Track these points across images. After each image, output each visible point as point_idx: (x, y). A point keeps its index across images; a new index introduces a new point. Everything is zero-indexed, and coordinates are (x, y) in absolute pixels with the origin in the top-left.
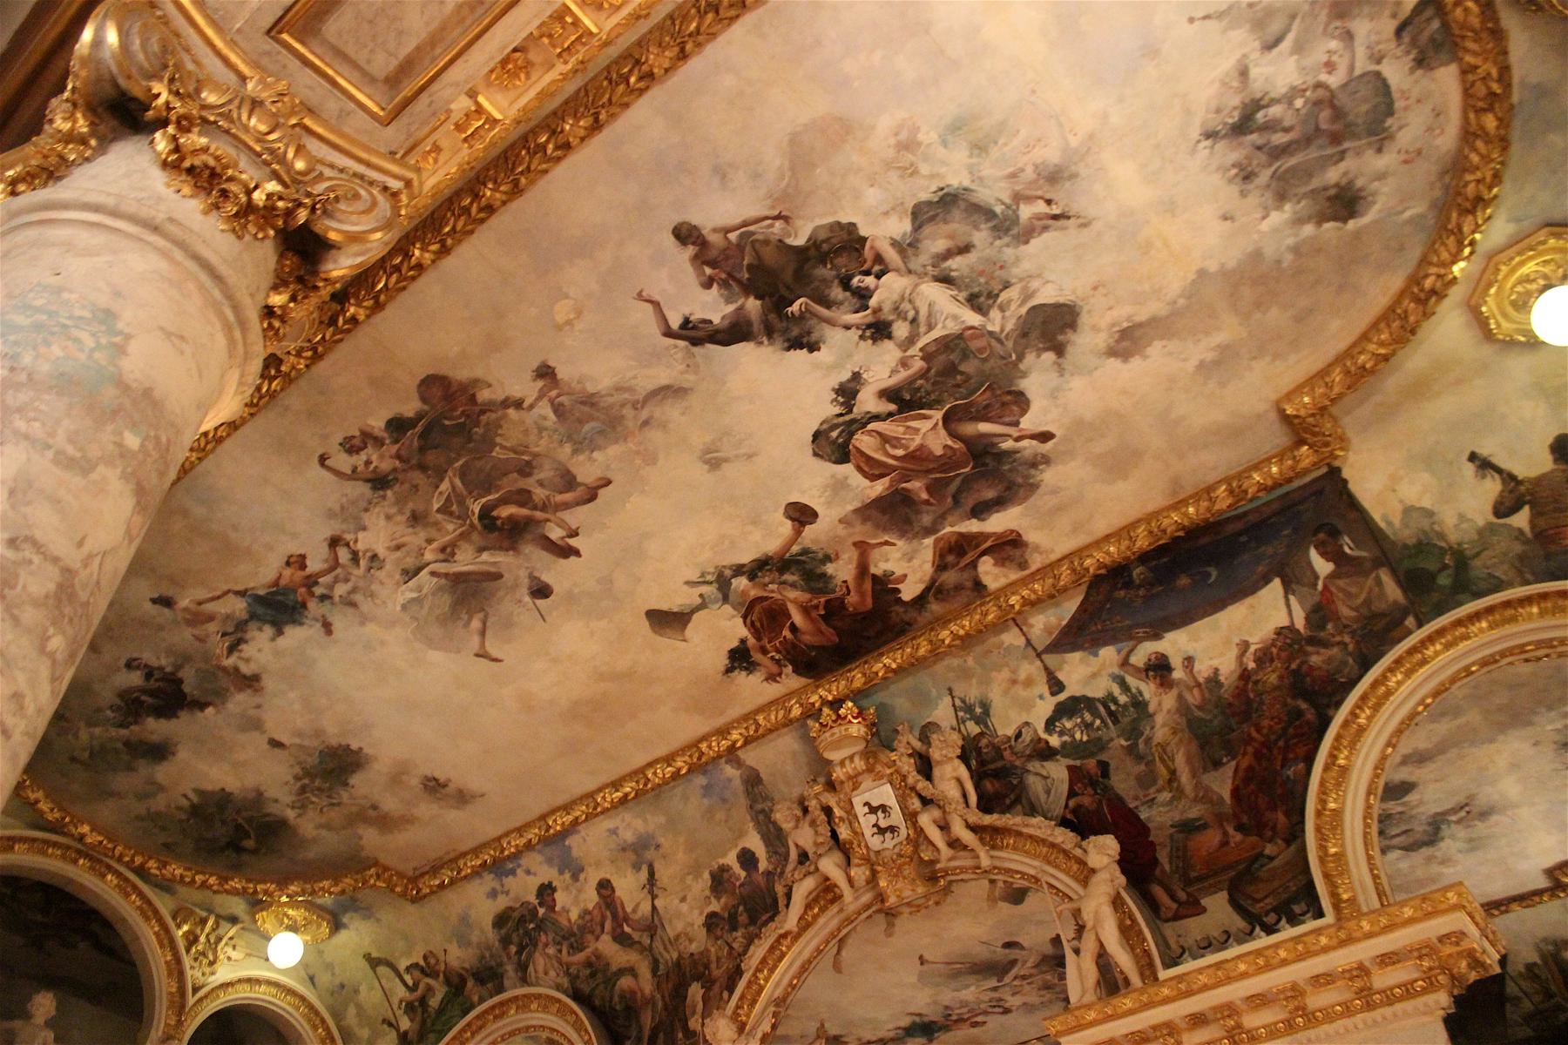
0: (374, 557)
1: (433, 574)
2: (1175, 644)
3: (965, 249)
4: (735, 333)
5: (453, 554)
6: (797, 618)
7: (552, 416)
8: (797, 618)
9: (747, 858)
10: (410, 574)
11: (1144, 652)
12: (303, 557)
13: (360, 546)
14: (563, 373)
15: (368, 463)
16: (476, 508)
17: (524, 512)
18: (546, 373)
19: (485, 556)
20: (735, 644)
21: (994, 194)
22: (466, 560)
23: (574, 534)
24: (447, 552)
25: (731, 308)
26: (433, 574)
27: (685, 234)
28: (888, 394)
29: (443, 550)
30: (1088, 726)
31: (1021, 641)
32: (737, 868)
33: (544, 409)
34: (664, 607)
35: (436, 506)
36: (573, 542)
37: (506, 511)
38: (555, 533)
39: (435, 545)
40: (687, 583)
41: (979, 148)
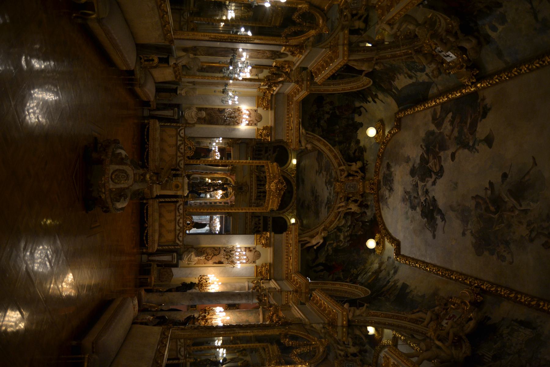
0: (528, 226)
1: (521, 206)
2: (410, 81)
3: (414, 197)
4: (440, 212)
5: (512, 207)
6: (469, 121)
7: (469, 223)
8: (469, 121)
9: (494, 29)
10: (526, 211)
11: (414, 80)
12: (543, 245)
13: (528, 232)
14: (461, 232)
15: (505, 251)
16: (496, 216)
17: (490, 205)
18: (464, 234)
19: (507, 199)
20: (483, 120)
21: (408, 204)
22: (511, 202)
23: (486, 189)
24: (512, 209)
25: (437, 217)
26: (521, 206)
27: (434, 236)
28: (431, 177)
29: (513, 211)
30: (417, 66)
31: (438, 86)
32: (497, 25)
33: (469, 227)
34: (487, 147)
35: (503, 225)
36: (488, 186)
37: (492, 209)
38: (489, 192)
39: (513, 214)
40: (478, 152)
41: (407, 213)
